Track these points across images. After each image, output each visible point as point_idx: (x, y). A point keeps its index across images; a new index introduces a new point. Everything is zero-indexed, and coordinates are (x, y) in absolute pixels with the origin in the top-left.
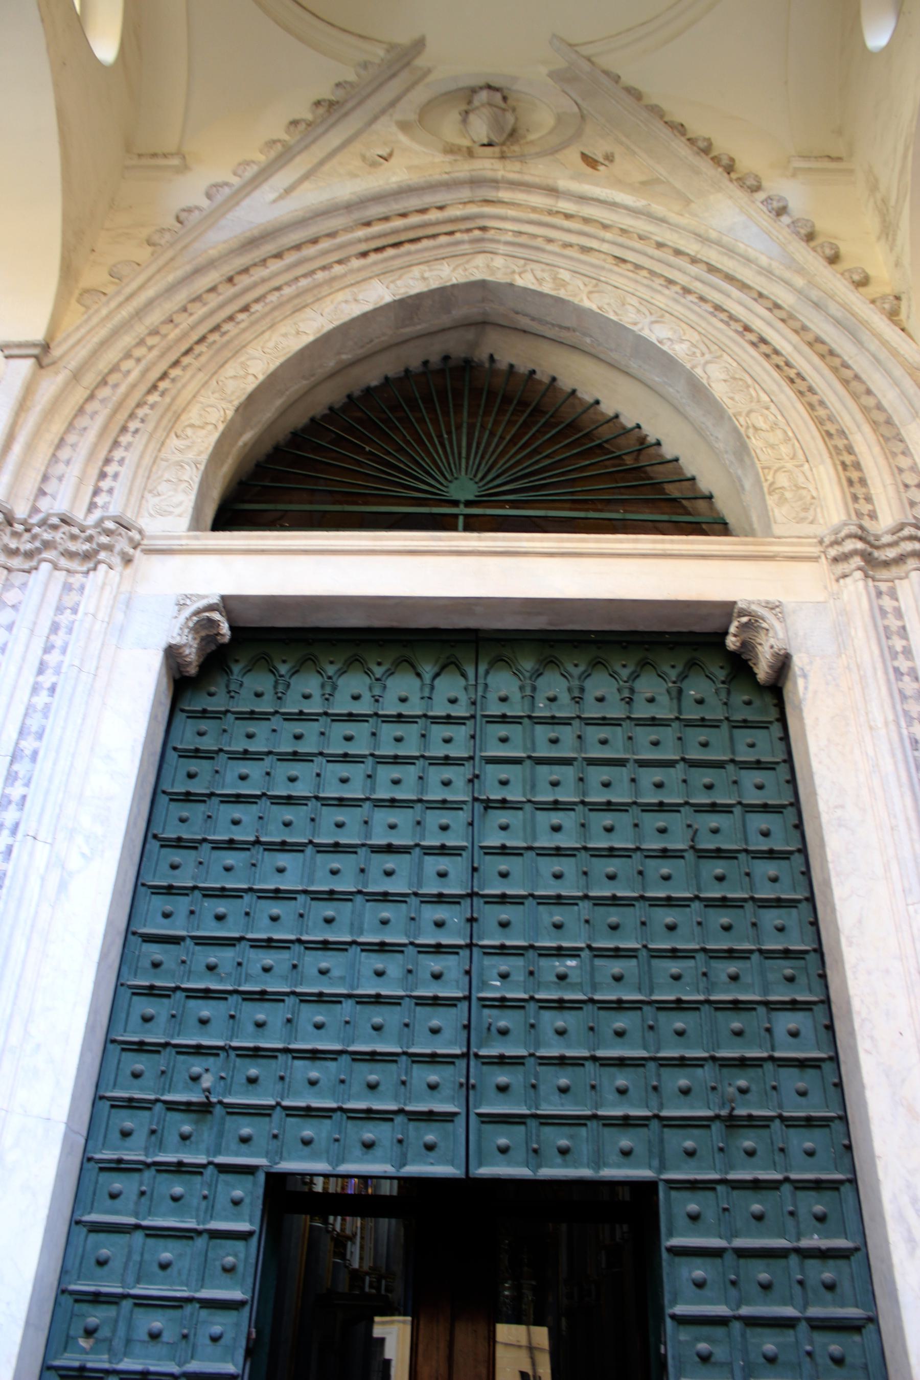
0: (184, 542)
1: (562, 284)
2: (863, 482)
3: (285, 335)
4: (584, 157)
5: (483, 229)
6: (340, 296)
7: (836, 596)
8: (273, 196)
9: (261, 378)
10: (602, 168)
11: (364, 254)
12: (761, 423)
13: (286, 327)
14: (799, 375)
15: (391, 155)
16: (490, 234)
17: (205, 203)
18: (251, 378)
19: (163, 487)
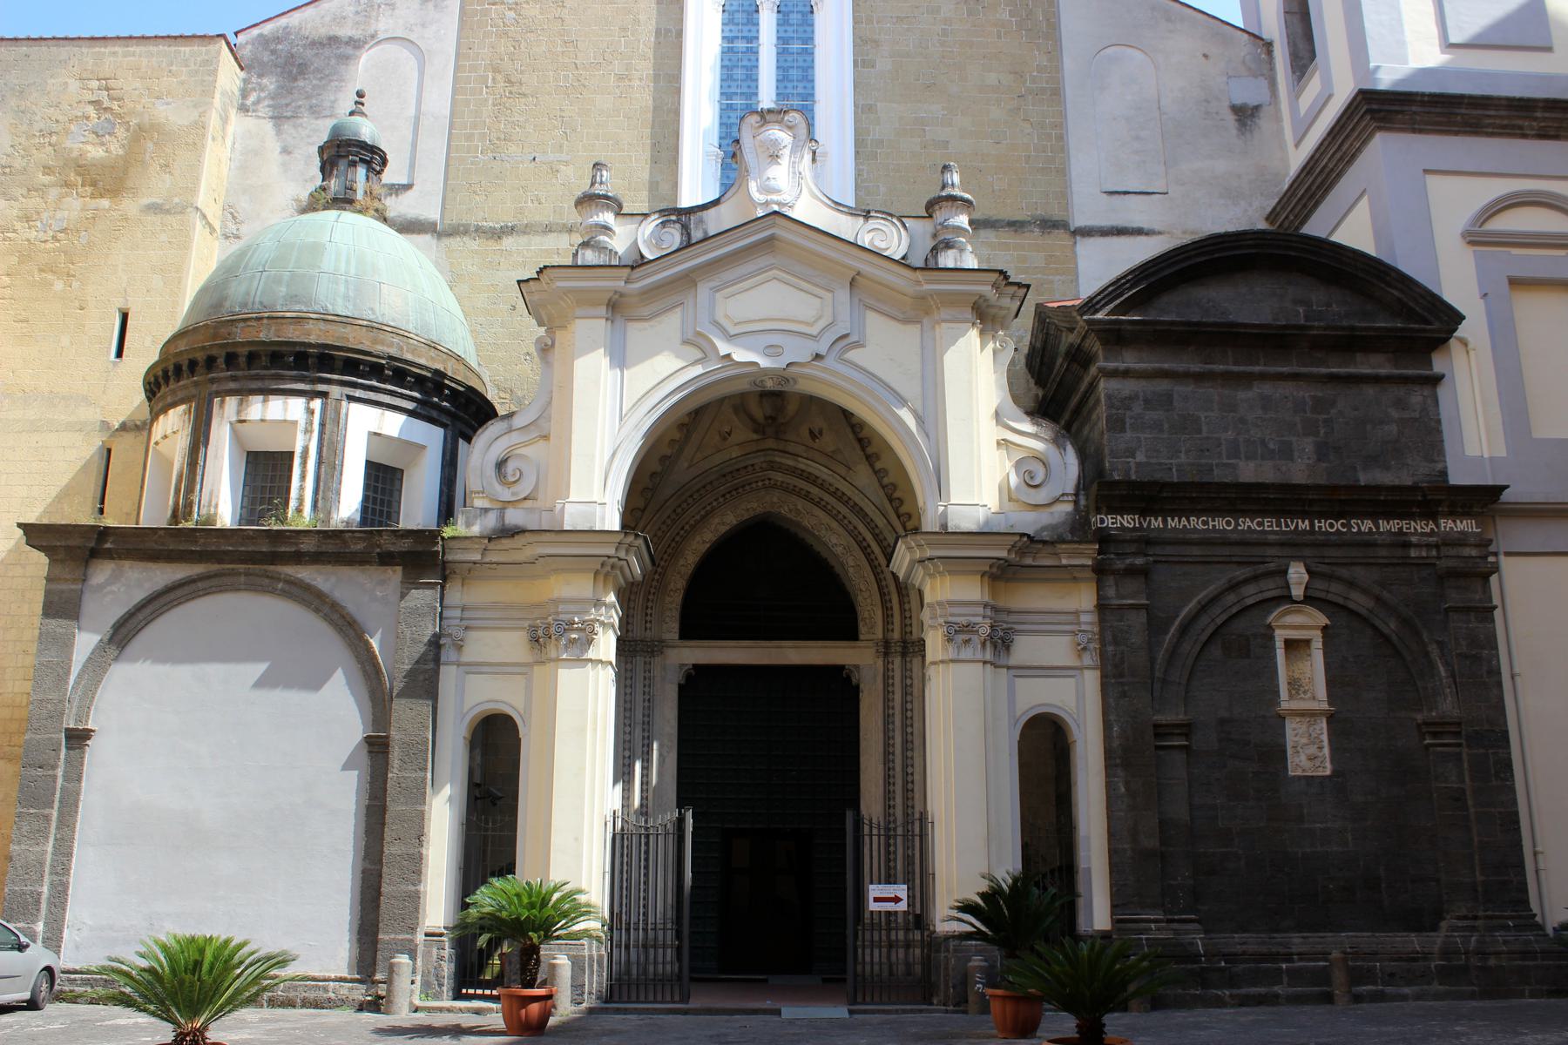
1: (798, 512)
2: (892, 615)
3: (698, 542)
4: (811, 432)
5: (770, 479)
6: (717, 521)
7: (875, 663)
8: (686, 465)
11: (723, 496)
13: (698, 538)
16: (772, 482)
17: (659, 469)
19: (667, 620)
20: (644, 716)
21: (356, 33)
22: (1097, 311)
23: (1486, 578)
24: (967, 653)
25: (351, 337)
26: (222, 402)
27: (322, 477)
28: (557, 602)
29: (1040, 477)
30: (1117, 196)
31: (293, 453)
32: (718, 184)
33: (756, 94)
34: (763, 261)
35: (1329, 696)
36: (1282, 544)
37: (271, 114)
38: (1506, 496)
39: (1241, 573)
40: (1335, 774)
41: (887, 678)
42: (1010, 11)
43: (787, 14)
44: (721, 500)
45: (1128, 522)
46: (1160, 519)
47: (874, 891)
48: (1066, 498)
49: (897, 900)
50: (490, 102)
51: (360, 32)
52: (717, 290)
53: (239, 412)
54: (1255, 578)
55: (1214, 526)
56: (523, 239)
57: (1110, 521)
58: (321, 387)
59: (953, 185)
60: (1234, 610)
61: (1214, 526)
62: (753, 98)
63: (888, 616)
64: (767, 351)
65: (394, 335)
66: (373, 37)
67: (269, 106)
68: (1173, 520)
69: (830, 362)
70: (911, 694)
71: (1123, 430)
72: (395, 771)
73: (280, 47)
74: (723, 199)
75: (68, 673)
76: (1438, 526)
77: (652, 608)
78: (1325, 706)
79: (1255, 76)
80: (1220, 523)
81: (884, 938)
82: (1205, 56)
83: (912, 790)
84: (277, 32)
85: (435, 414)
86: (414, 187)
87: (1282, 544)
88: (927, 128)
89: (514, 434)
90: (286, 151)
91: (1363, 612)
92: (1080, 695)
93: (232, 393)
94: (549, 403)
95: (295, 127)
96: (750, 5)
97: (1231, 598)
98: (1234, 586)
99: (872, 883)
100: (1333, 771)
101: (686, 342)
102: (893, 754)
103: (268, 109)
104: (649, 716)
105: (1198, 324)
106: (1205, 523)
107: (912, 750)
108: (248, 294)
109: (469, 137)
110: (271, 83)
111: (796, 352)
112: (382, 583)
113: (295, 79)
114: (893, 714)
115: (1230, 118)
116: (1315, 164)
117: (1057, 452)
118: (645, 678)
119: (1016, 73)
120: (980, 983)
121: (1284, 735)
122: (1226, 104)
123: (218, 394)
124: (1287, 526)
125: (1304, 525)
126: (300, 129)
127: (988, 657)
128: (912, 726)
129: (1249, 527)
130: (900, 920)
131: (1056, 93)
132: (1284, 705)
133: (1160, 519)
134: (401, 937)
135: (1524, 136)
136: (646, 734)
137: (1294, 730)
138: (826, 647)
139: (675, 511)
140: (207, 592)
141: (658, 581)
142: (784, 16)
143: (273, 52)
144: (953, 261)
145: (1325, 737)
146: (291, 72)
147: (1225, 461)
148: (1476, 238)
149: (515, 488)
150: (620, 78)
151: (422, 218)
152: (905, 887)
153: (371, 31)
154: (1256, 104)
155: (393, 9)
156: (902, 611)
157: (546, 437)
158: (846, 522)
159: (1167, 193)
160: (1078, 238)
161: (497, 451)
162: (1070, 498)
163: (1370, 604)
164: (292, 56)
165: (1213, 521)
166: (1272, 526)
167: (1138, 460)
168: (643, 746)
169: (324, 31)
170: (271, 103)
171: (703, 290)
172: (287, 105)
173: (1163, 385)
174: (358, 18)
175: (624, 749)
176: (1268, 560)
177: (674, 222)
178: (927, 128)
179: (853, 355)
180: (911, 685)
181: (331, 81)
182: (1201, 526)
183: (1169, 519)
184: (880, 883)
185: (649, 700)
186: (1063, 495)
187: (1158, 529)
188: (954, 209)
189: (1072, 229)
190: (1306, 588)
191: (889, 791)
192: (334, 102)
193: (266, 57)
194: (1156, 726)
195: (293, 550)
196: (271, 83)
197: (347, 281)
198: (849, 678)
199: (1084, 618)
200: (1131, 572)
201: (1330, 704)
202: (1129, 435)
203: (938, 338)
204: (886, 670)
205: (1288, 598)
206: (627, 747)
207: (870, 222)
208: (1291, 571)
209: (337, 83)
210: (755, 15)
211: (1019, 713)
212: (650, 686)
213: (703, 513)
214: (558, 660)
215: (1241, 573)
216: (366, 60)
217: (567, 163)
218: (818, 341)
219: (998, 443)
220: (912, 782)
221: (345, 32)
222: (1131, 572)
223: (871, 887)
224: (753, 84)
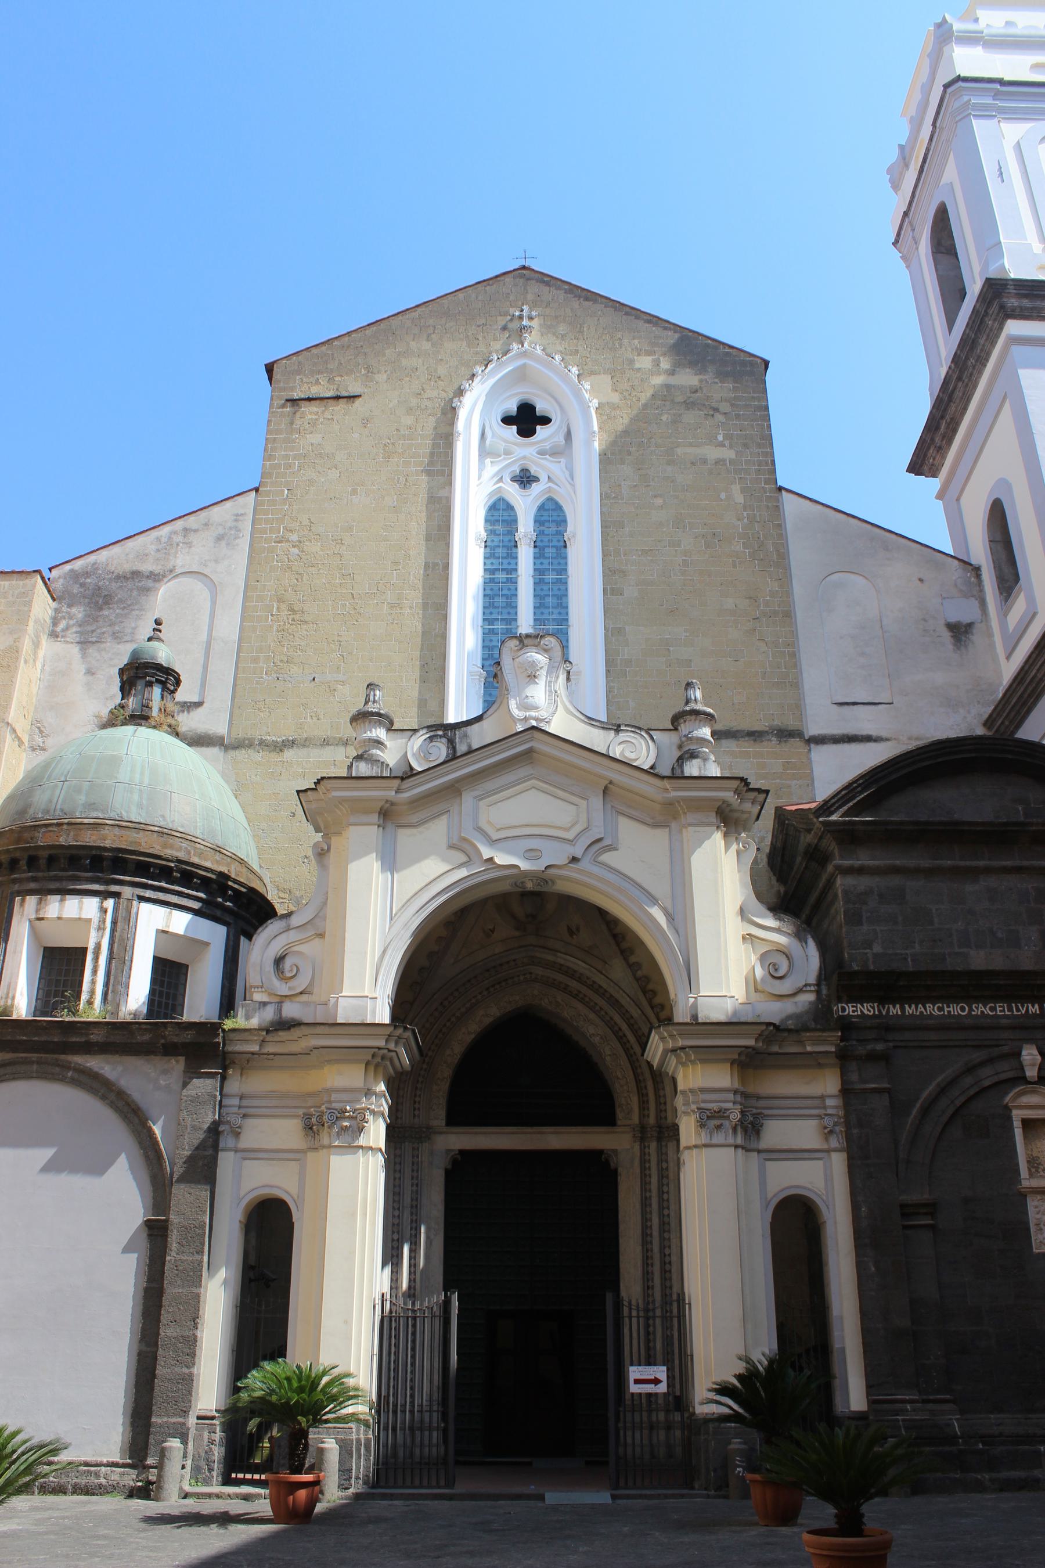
0: (445, 1130)
4: (569, 928)
5: (531, 973)
9: (459, 1056)
10: (575, 937)
11: (487, 989)
12: (620, 1076)
14: (634, 1053)
15: (494, 928)
18: (455, 1056)
20: (412, 1200)
21: (157, 569)
22: (831, 813)
24: (719, 1138)
25: (143, 841)
26: (23, 901)
27: (113, 972)
28: (329, 1091)
30: (846, 707)
31: (86, 948)
32: (481, 701)
33: (516, 620)
34: (523, 772)
36: (1014, 1028)
37: (78, 639)
39: (977, 1056)
41: (644, 1161)
42: (743, 543)
43: (542, 549)
44: (485, 993)
45: (868, 1010)
46: (898, 1006)
47: (635, 1372)
48: (808, 988)
49: (656, 1381)
50: (275, 628)
51: (160, 567)
52: (480, 798)
53: (37, 911)
54: (991, 1061)
55: (949, 1012)
56: (303, 752)
57: (851, 1009)
58: (114, 888)
59: (696, 700)
60: (972, 1092)
61: (949, 1012)
62: (513, 623)
63: (643, 1102)
64: (527, 855)
65: (183, 840)
66: (171, 571)
67: (76, 632)
68: (910, 1007)
69: (585, 864)
70: (667, 1177)
71: (860, 923)
72: (173, 1254)
73: (88, 580)
74: (485, 716)
77: (420, 1096)
79: (966, 597)
80: (955, 1009)
81: (645, 1419)
82: (921, 580)
83: (670, 1271)
85: (218, 913)
86: (205, 705)
87: (1014, 1028)
88: (671, 649)
89: (291, 932)
90: (90, 672)
92: (828, 1178)
94: (325, 903)
96: (510, 541)
97: (968, 1080)
98: (970, 1069)
99: (632, 1365)
101: (451, 847)
102: (651, 1235)
103: (75, 635)
104: (417, 1200)
105: (927, 823)
106: (940, 1009)
107: (669, 1232)
108: (50, 801)
109: (255, 660)
110: (79, 612)
111: (554, 855)
112: (165, 1072)
113: (101, 609)
114: (650, 1197)
115: (946, 635)
116: (1025, 674)
117: (799, 945)
118: (413, 1163)
119: (751, 598)
120: (739, 1466)
121: (1026, 1213)
122: (943, 622)
123: (19, 893)
124: (1018, 1010)
127: (739, 1141)
128: (668, 1208)
129: (982, 1012)
130: (661, 1401)
131: (788, 615)
132: (1025, 1183)
133: (898, 1006)
134: (173, 1420)
136: (414, 1218)
137: (1036, 1207)
138: (585, 1133)
139: (442, 1003)
141: (425, 1070)
142: (540, 550)
143: (82, 585)
144: (698, 769)
146: (97, 602)
147: (957, 950)
149: (291, 983)
150: (392, 606)
151: (211, 732)
152: (664, 1368)
153: (170, 566)
154: (969, 621)
155: (190, 547)
156: (657, 1097)
157: (321, 935)
158: (603, 1013)
159: (892, 703)
160: (812, 746)
161: (276, 948)
162: (812, 988)
164: (99, 588)
165: (948, 1007)
166: (1004, 1011)
167: (875, 951)
168: (411, 1229)
169: (128, 567)
170: (79, 629)
171: (468, 798)
172: (93, 631)
173: (895, 881)
175: (393, 1232)
177: (441, 737)
178: (671, 649)
179: (606, 858)
180: (667, 1169)
181: (132, 610)
182: (936, 1012)
183: (907, 1006)
184: (640, 1365)
185: (417, 1185)
186: (806, 985)
188: (697, 722)
189: (807, 738)
190: (1040, 1069)
191: (648, 1272)
192: (134, 628)
193: (76, 589)
194: (903, 1206)
195: (83, 1040)
196: (79, 612)
197: (140, 790)
198: (607, 1162)
199: (830, 1102)
200: (873, 1057)
202: (865, 928)
204: (643, 1153)
206: (395, 1230)
207: (621, 734)
208: (1024, 1053)
209: (137, 612)
210: (514, 550)
211: (770, 1195)
212: (417, 1171)
213: (468, 1005)
214: (330, 1147)
215: (977, 1056)
216: (163, 591)
217: (343, 683)
218: (574, 845)
219: (744, 938)
220: (670, 1263)
221: (146, 567)
222: (873, 1057)
223: (631, 1369)
224: (512, 611)
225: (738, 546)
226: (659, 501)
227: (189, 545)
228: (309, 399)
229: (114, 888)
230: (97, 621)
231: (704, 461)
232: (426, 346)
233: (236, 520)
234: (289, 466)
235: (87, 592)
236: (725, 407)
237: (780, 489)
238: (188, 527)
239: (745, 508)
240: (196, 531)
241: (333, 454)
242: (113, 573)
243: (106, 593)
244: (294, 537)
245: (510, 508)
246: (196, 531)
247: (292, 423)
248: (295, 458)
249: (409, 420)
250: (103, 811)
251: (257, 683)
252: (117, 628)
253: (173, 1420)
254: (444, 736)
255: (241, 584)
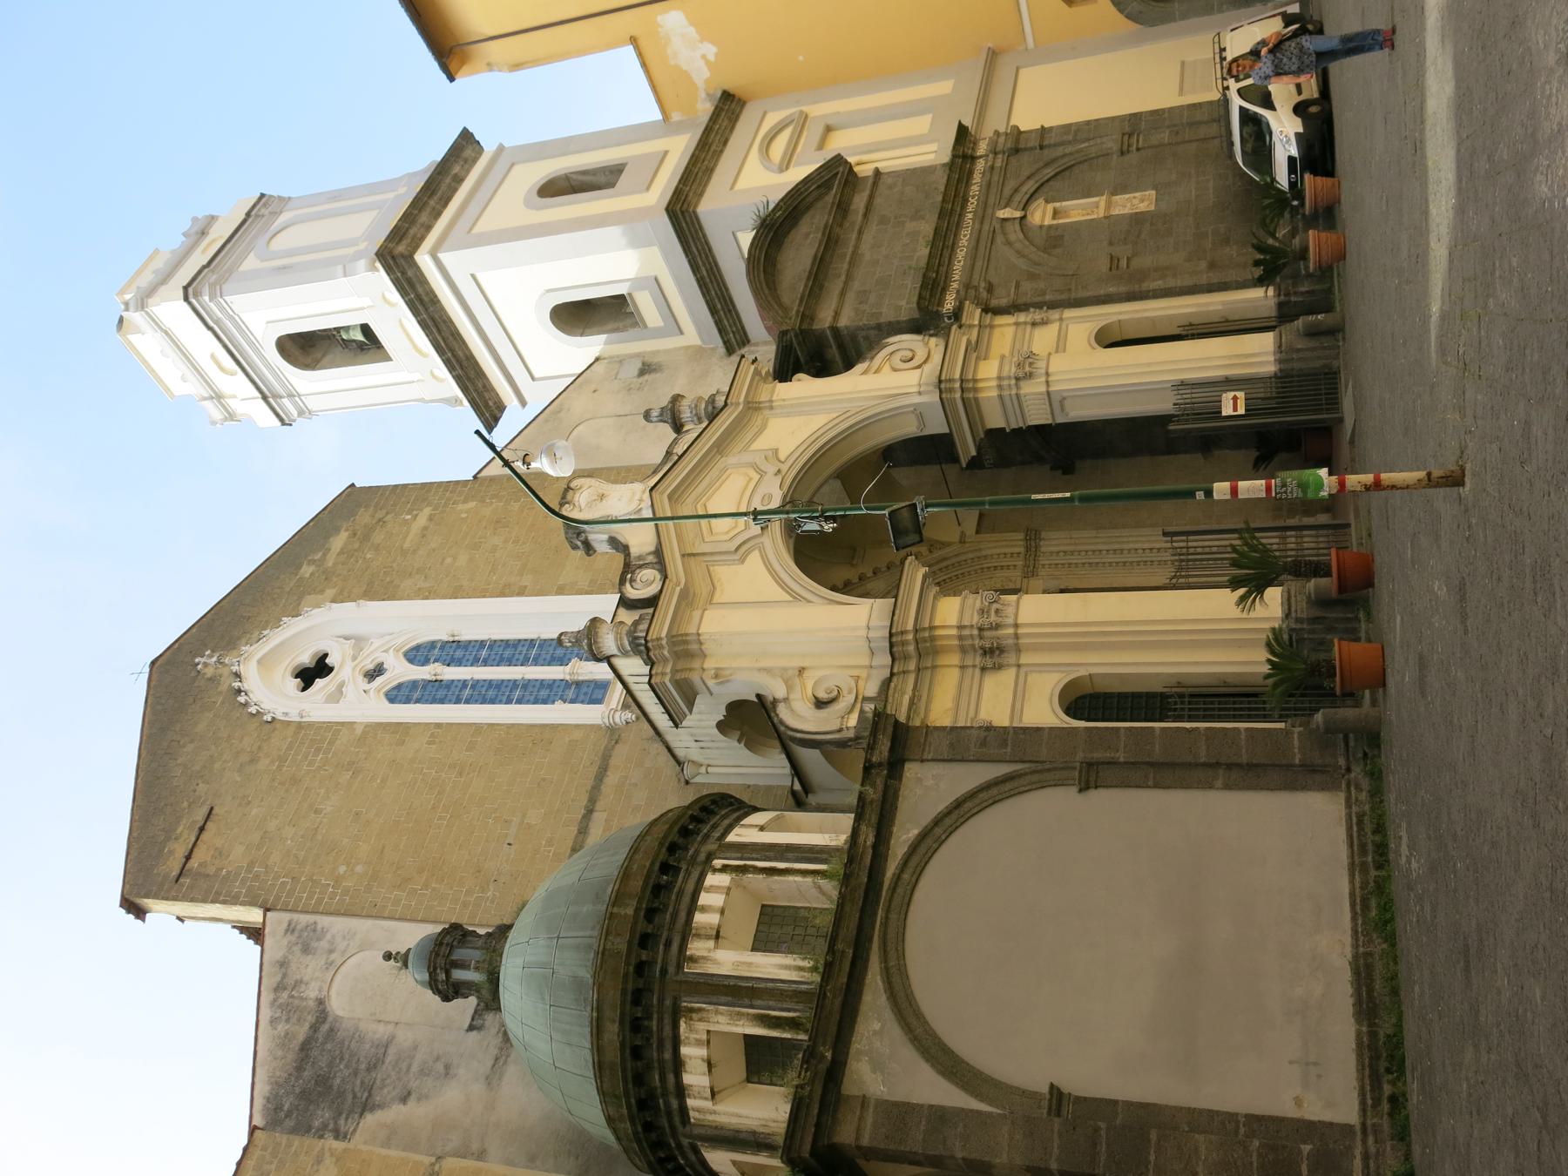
21: (310, 1019)
23: (1020, 132)
26: (693, 959)
29: (909, 354)
35: (1097, 196)
37: (356, 1116)
38: (967, 122)
40: (1155, 187)
53: (708, 937)
58: (702, 857)
67: (347, 1119)
72: (1117, 755)
73: (286, 1108)
75: (979, 1113)
76: (981, 157)
78: (1104, 197)
80: (961, 254)
84: (268, 1109)
90: (404, 1099)
91: (1037, 185)
93: (683, 946)
95: (381, 1089)
100: (1153, 189)
101: (742, 561)
106: (959, 261)
110: (322, 1117)
115: (646, 377)
122: (635, 380)
123: (679, 967)
125: (970, 216)
126: (388, 1081)
134: (1296, 742)
135: (722, 151)
140: (901, 955)
145: (1127, 196)
148: (785, 166)
149: (845, 692)
150: (460, 774)
155: (301, 982)
157: (801, 671)
163: (1031, 183)
164: (303, 1092)
169: (291, 1056)
170: (344, 1116)
172: (355, 1097)
173: (851, 296)
174: (294, 1020)
176: (992, 229)
182: (962, 263)
187: (959, 285)
194: (1111, 269)
196: (322, 1117)
201: (1102, 195)
203: (782, 403)
205: (1023, 218)
208: (1002, 217)
215: (999, 239)
217: (524, 816)
221: (302, 1032)
225: (516, 506)
226: (449, 560)
227: (298, 983)
228: (188, 858)
229: (702, 857)
230: (344, 1092)
231: (425, 528)
232: (190, 748)
233: (293, 931)
234: (257, 876)
235: (300, 1108)
236: (379, 515)
237: (475, 477)
238: (275, 985)
239: (484, 502)
240: (284, 976)
241: (265, 832)
242: (290, 1075)
243: (313, 1082)
244: (342, 869)
245: (399, 687)
246: (284, 976)
247: (208, 875)
248: (249, 870)
249: (263, 764)
250: (609, 884)
251: (492, 902)
252: (363, 1066)
253: (1296, 742)
254: (633, 572)
255: (369, 923)
